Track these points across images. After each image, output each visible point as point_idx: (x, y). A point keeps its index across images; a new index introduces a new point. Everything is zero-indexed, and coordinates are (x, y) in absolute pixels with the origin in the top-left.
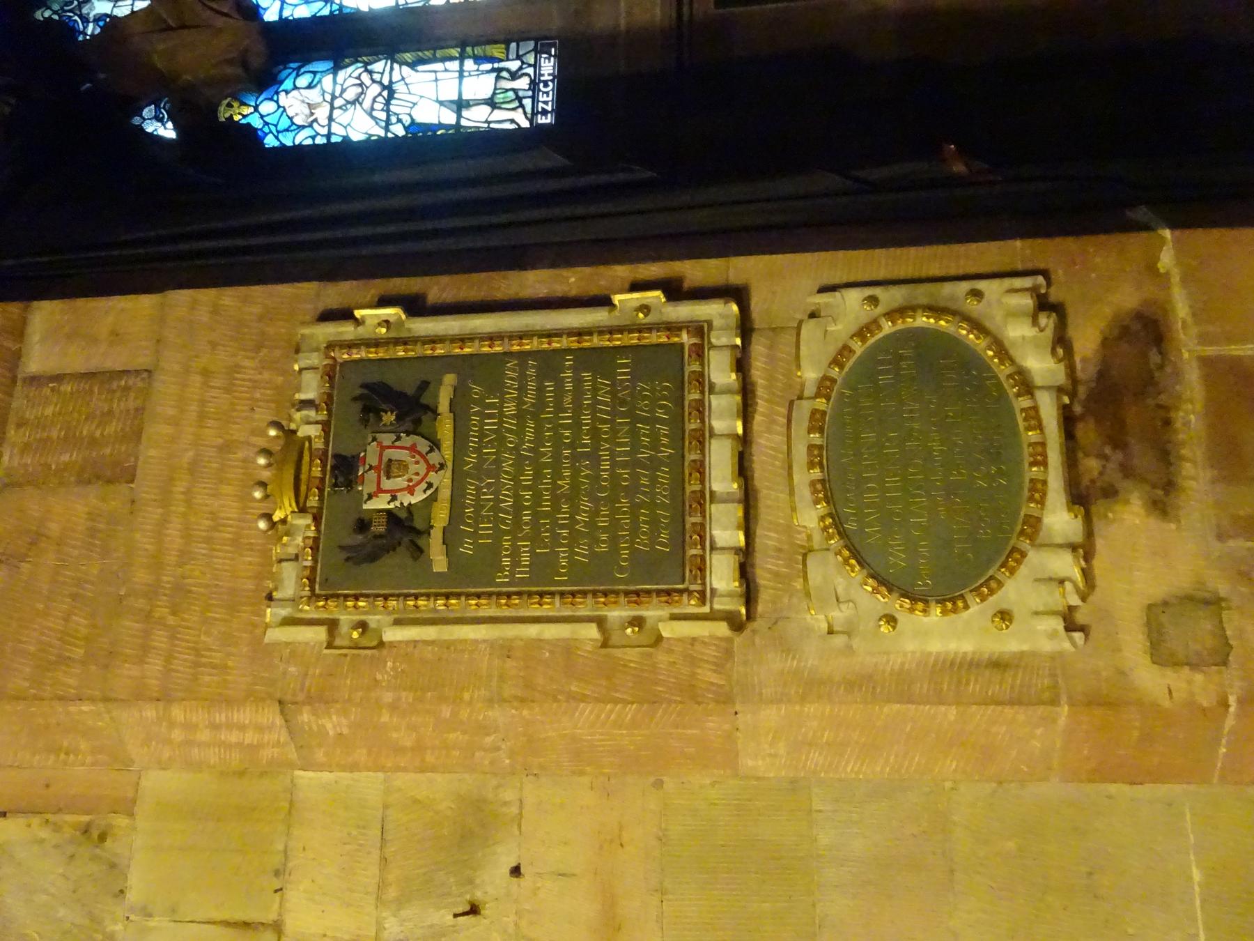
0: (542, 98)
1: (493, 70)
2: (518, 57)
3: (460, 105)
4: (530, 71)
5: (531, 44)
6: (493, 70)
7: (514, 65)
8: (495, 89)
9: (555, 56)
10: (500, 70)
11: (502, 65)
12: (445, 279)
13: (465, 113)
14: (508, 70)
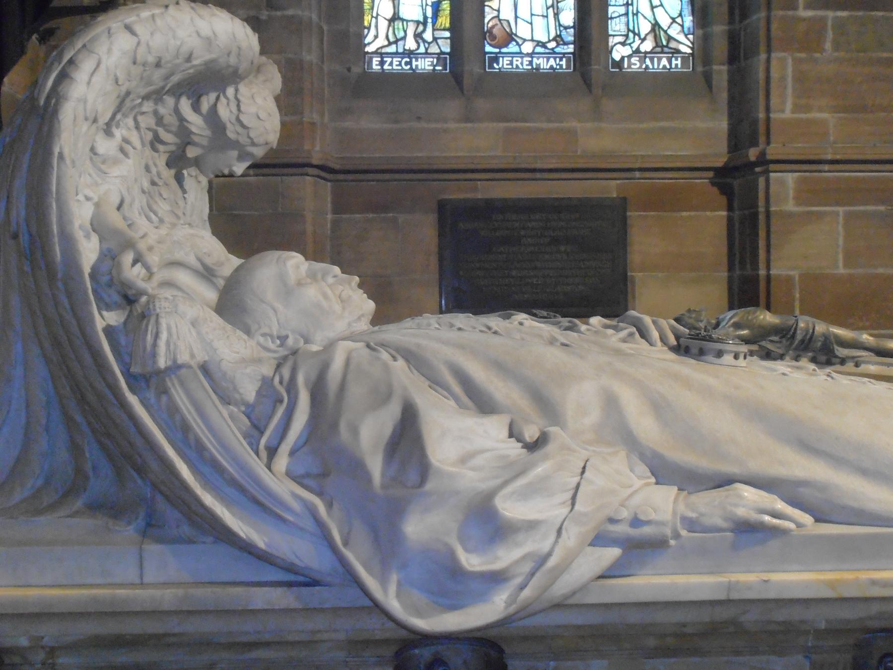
0: (396, 61)
1: (425, 18)
2: (435, 39)
4: (422, 50)
5: (447, 49)
6: (425, 18)
7: (428, 36)
8: (407, 21)
9: (434, 70)
10: (425, 24)
11: (430, 26)
14: (424, 31)
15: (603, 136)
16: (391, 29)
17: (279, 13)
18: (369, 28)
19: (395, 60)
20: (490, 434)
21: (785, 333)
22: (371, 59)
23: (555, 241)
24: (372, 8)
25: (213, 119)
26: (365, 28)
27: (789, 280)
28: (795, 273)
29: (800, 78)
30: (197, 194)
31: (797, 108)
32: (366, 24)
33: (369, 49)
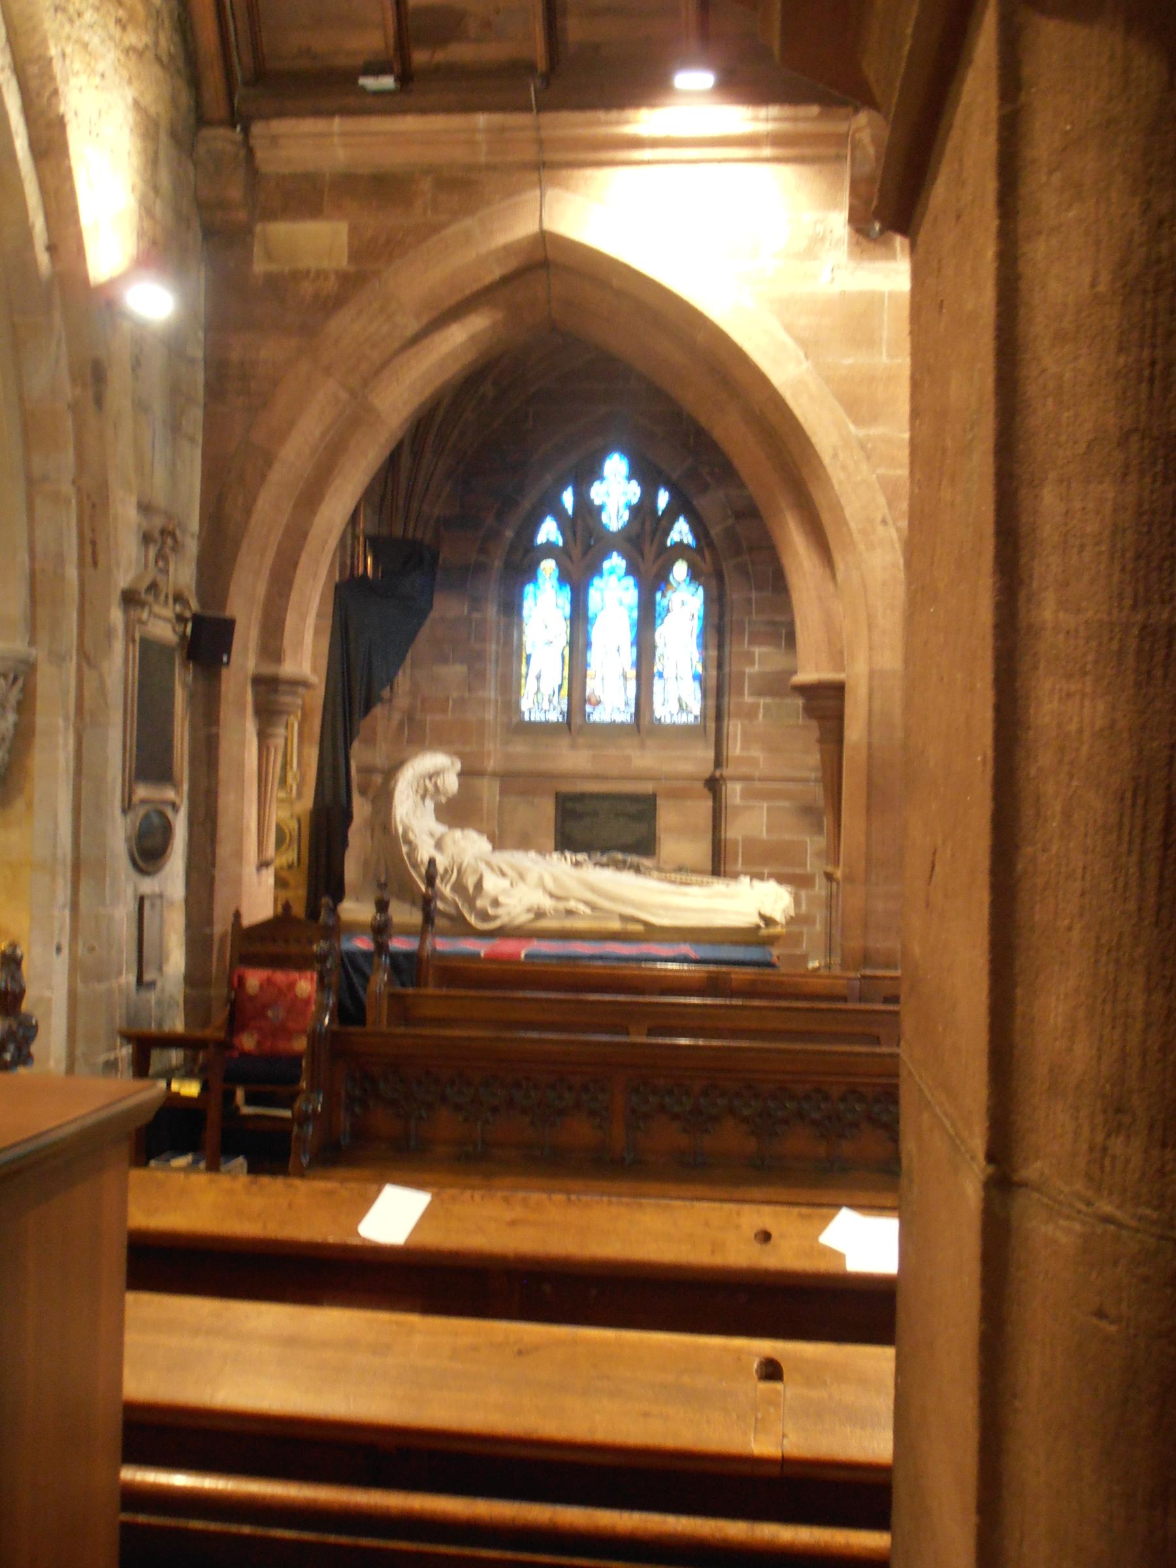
3: (538, 678)
15: (646, 760)
20: (505, 883)
21: (624, 862)
23: (617, 815)
25: (436, 785)
27: (736, 842)
28: (740, 838)
29: (745, 734)
30: (430, 804)
31: (742, 748)
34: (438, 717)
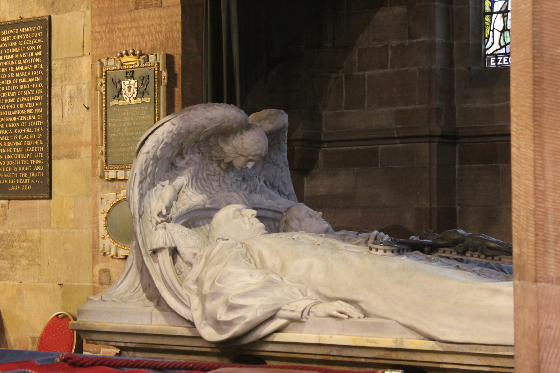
12: (180, 93)
13: (500, 16)
16: (502, 37)
17: (415, 41)
18: (488, 38)
19: (504, 58)
22: (490, 58)
24: (490, 25)
26: (485, 38)
32: (487, 35)
33: (489, 52)
34: (377, 72)
